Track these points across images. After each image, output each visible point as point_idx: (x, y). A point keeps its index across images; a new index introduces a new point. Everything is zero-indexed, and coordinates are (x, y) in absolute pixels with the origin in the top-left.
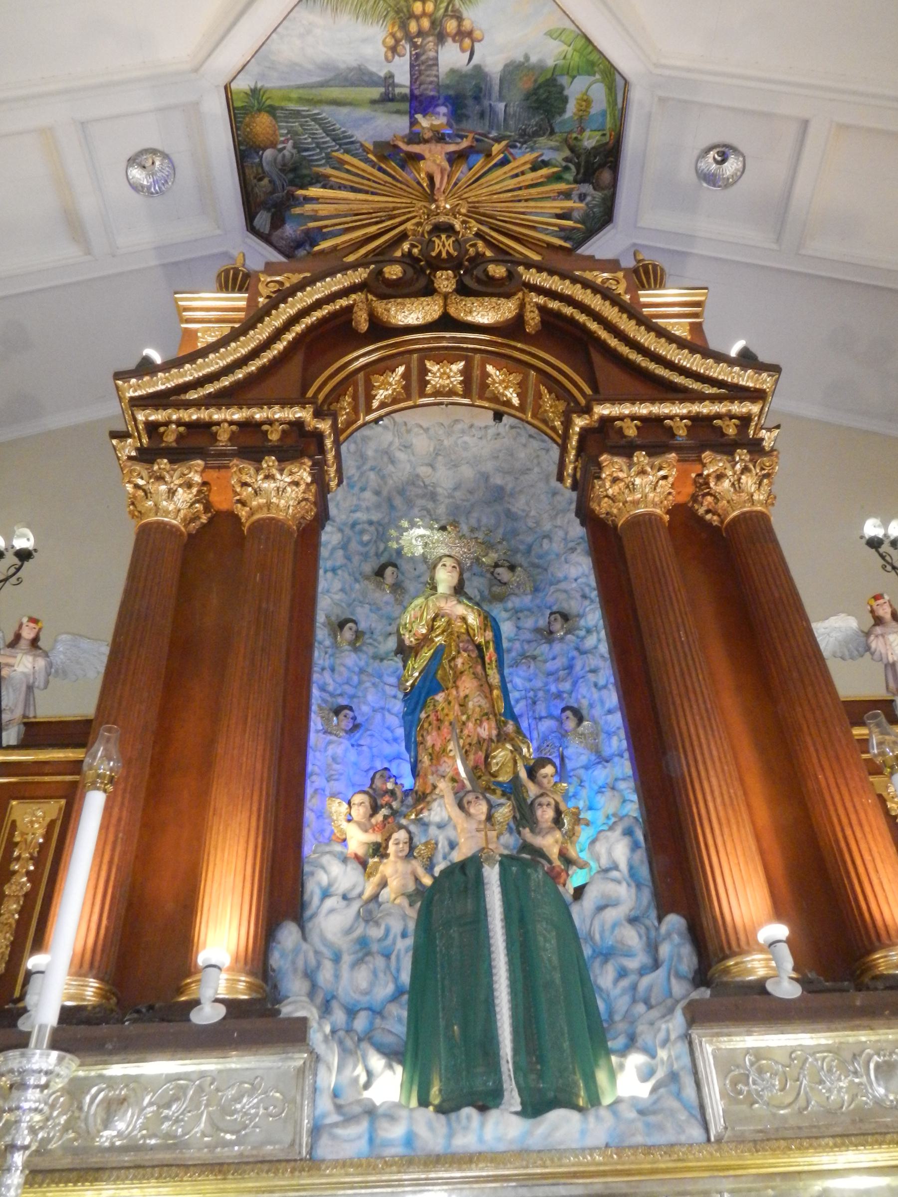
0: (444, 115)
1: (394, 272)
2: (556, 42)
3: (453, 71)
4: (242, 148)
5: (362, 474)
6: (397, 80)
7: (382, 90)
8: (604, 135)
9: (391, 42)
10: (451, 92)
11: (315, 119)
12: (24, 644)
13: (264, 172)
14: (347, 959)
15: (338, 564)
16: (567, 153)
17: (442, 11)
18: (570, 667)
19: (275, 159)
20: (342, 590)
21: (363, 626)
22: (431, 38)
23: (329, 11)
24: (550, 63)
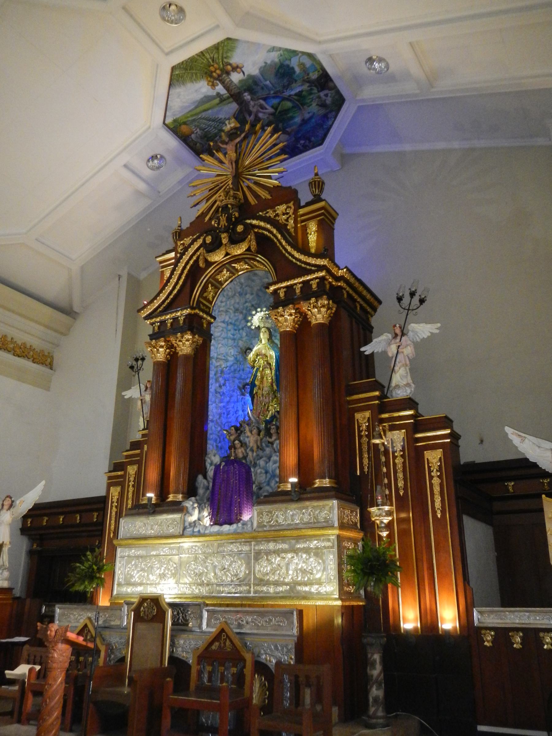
0: (248, 95)
1: (209, 239)
2: (274, 53)
3: (241, 81)
4: (183, 138)
5: (243, 290)
8: (319, 71)
9: (211, 84)
10: (245, 87)
11: (200, 118)
13: (195, 142)
15: (243, 326)
16: (308, 84)
17: (221, 66)
19: (197, 137)
20: (247, 335)
22: (224, 75)
23: (181, 85)
24: (277, 60)
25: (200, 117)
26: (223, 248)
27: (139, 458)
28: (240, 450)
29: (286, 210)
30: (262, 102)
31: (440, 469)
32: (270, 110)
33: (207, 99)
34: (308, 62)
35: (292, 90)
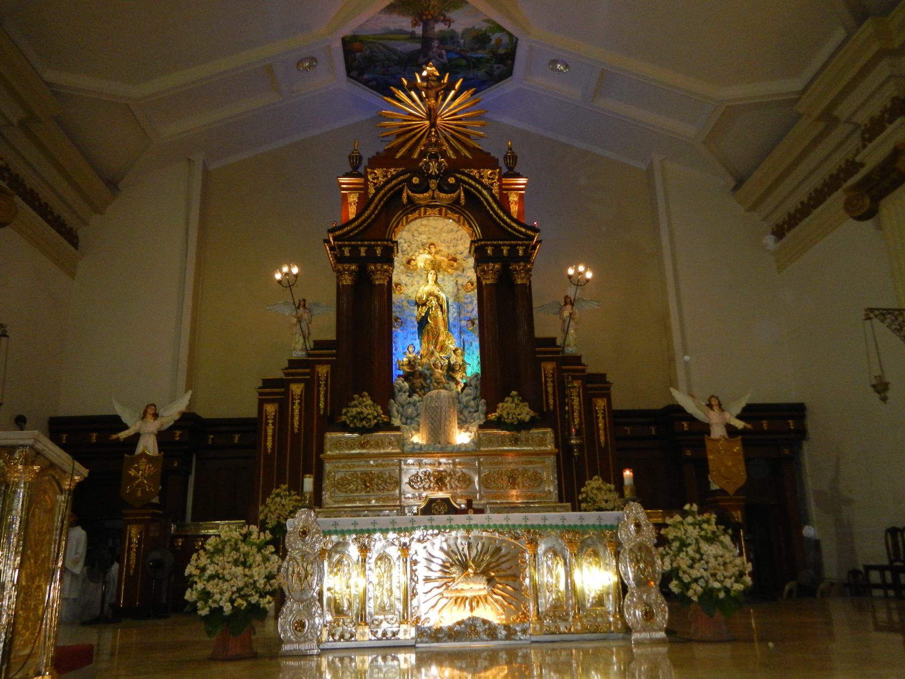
1: (416, 180)
3: (441, 31)
6: (417, 33)
7: (409, 36)
11: (381, 44)
12: (301, 308)
14: (405, 407)
16: (491, 55)
17: (436, 14)
18: (471, 302)
21: (404, 282)
24: (484, 29)
25: (380, 41)
26: (430, 192)
27: (309, 377)
28: (419, 380)
29: (491, 174)
30: (444, 52)
31: (604, 413)
32: (445, 60)
33: (401, 32)
34: (505, 39)
35: (476, 54)
